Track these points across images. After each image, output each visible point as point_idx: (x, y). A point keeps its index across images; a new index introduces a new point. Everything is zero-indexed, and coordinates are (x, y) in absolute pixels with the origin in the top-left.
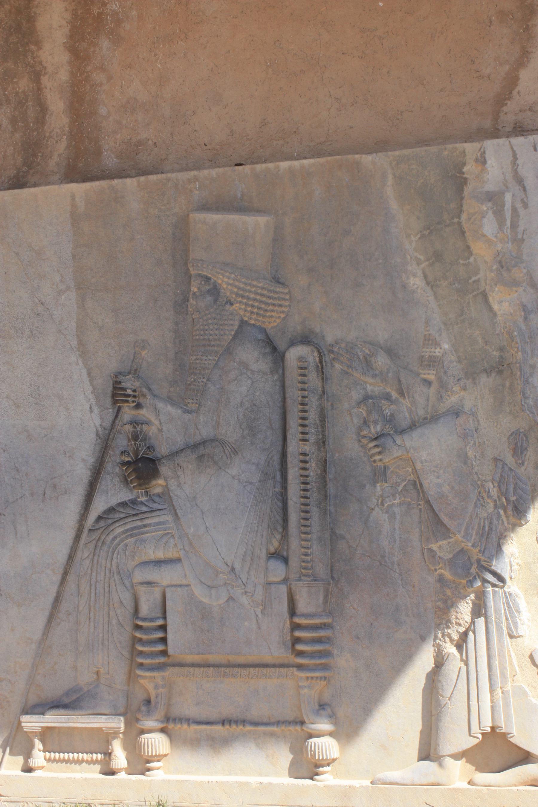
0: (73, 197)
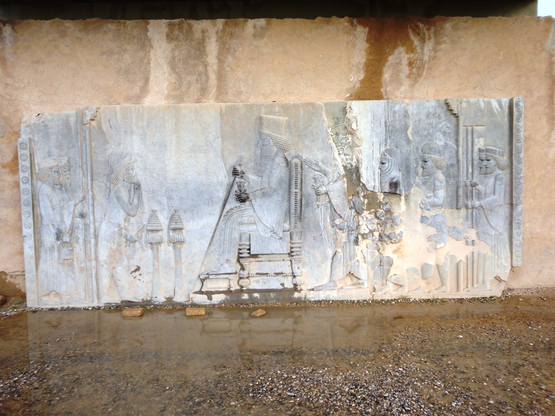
0: (221, 107)
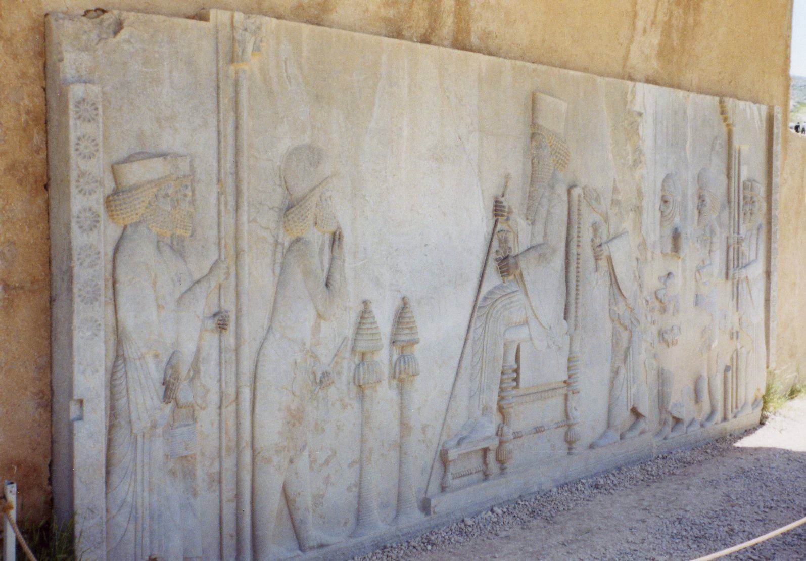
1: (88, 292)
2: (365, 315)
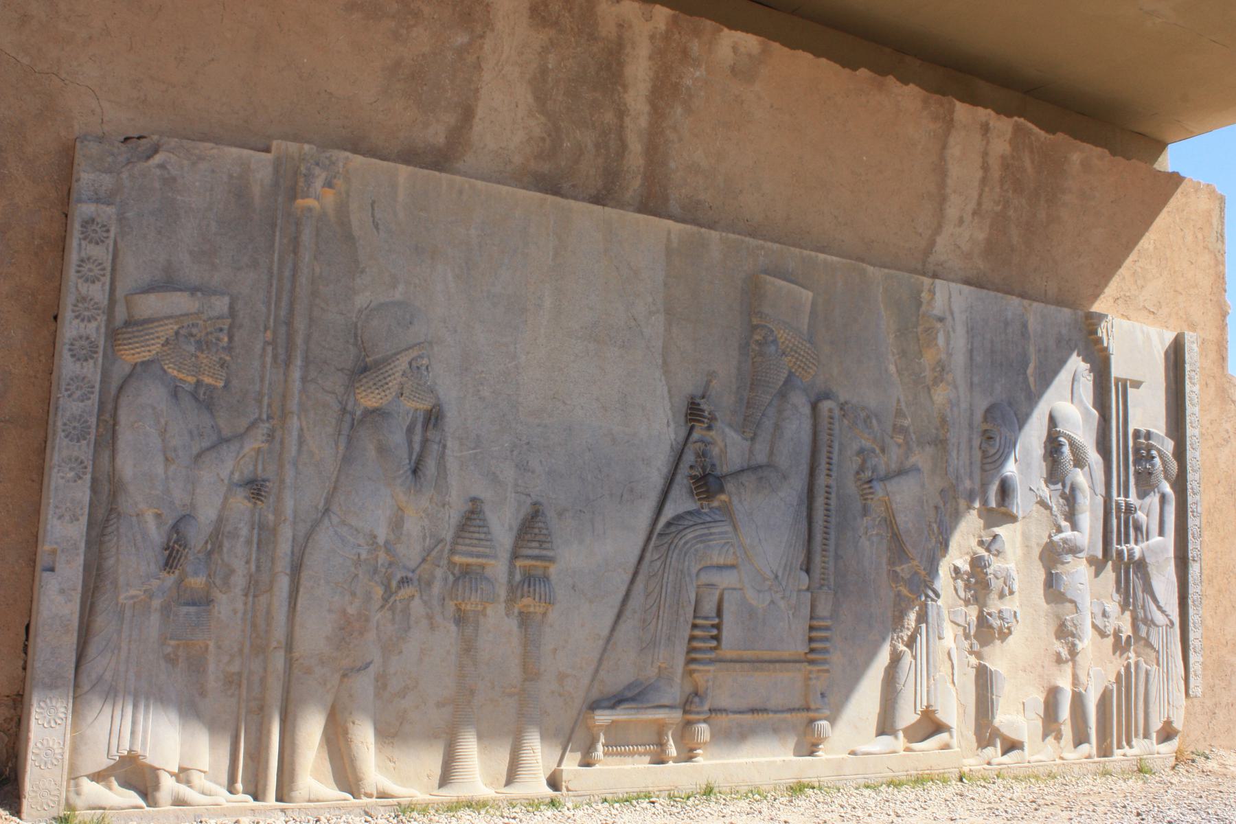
0: (669, 233)
1: (74, 428)
2: (473, 517)
